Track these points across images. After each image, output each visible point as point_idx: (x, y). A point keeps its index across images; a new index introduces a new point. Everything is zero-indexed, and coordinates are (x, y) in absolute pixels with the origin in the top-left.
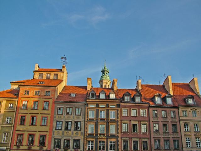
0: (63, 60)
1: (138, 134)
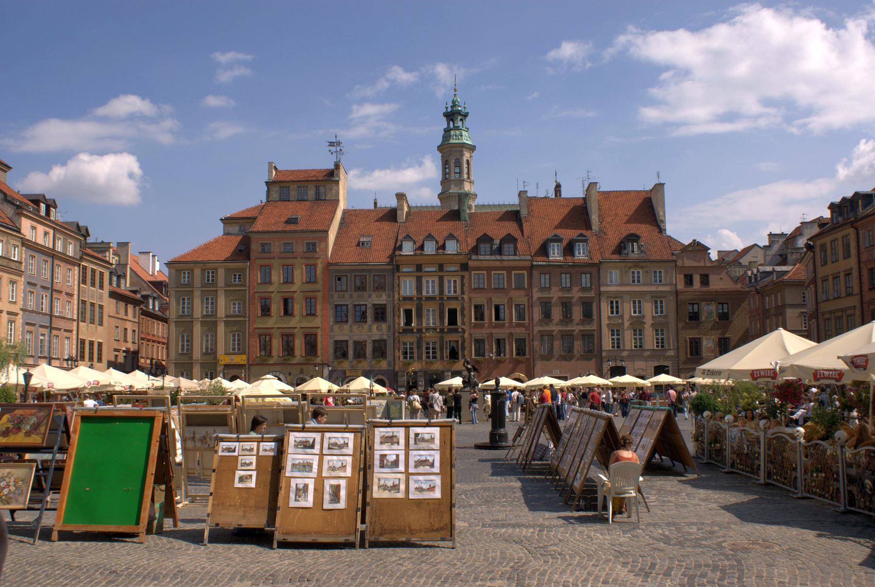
0: (333, 149)
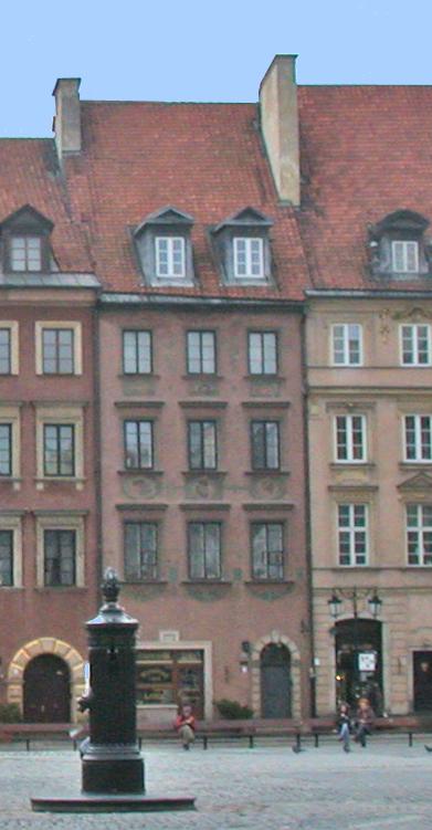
1: (17, 486)
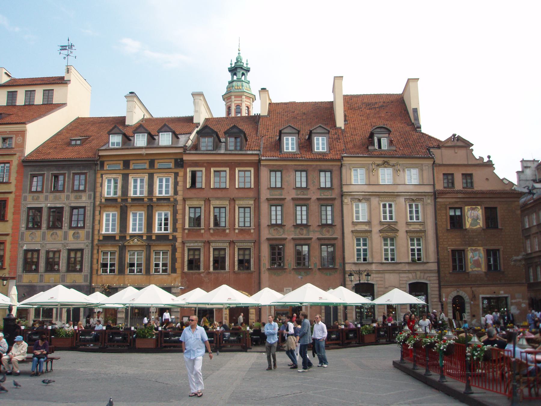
1: (227, 231)
